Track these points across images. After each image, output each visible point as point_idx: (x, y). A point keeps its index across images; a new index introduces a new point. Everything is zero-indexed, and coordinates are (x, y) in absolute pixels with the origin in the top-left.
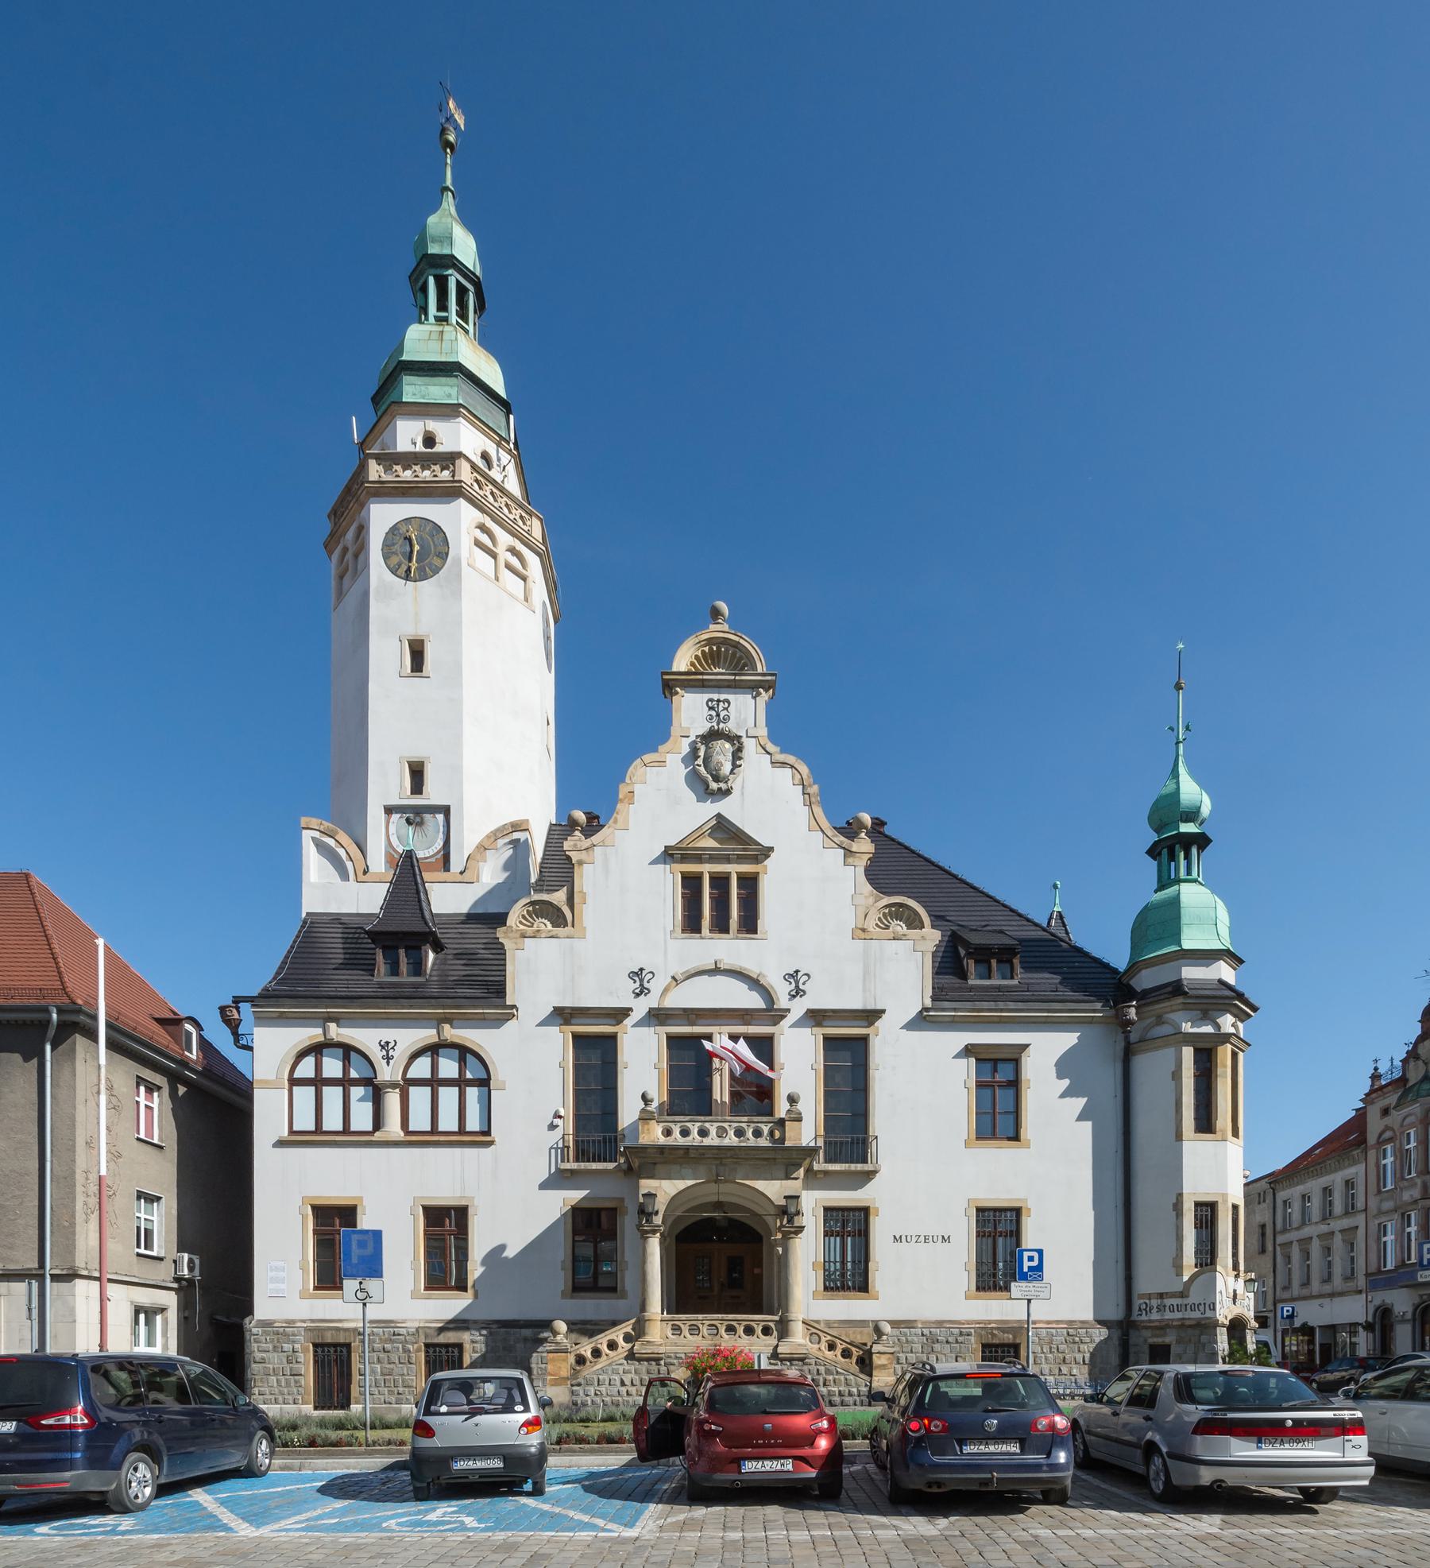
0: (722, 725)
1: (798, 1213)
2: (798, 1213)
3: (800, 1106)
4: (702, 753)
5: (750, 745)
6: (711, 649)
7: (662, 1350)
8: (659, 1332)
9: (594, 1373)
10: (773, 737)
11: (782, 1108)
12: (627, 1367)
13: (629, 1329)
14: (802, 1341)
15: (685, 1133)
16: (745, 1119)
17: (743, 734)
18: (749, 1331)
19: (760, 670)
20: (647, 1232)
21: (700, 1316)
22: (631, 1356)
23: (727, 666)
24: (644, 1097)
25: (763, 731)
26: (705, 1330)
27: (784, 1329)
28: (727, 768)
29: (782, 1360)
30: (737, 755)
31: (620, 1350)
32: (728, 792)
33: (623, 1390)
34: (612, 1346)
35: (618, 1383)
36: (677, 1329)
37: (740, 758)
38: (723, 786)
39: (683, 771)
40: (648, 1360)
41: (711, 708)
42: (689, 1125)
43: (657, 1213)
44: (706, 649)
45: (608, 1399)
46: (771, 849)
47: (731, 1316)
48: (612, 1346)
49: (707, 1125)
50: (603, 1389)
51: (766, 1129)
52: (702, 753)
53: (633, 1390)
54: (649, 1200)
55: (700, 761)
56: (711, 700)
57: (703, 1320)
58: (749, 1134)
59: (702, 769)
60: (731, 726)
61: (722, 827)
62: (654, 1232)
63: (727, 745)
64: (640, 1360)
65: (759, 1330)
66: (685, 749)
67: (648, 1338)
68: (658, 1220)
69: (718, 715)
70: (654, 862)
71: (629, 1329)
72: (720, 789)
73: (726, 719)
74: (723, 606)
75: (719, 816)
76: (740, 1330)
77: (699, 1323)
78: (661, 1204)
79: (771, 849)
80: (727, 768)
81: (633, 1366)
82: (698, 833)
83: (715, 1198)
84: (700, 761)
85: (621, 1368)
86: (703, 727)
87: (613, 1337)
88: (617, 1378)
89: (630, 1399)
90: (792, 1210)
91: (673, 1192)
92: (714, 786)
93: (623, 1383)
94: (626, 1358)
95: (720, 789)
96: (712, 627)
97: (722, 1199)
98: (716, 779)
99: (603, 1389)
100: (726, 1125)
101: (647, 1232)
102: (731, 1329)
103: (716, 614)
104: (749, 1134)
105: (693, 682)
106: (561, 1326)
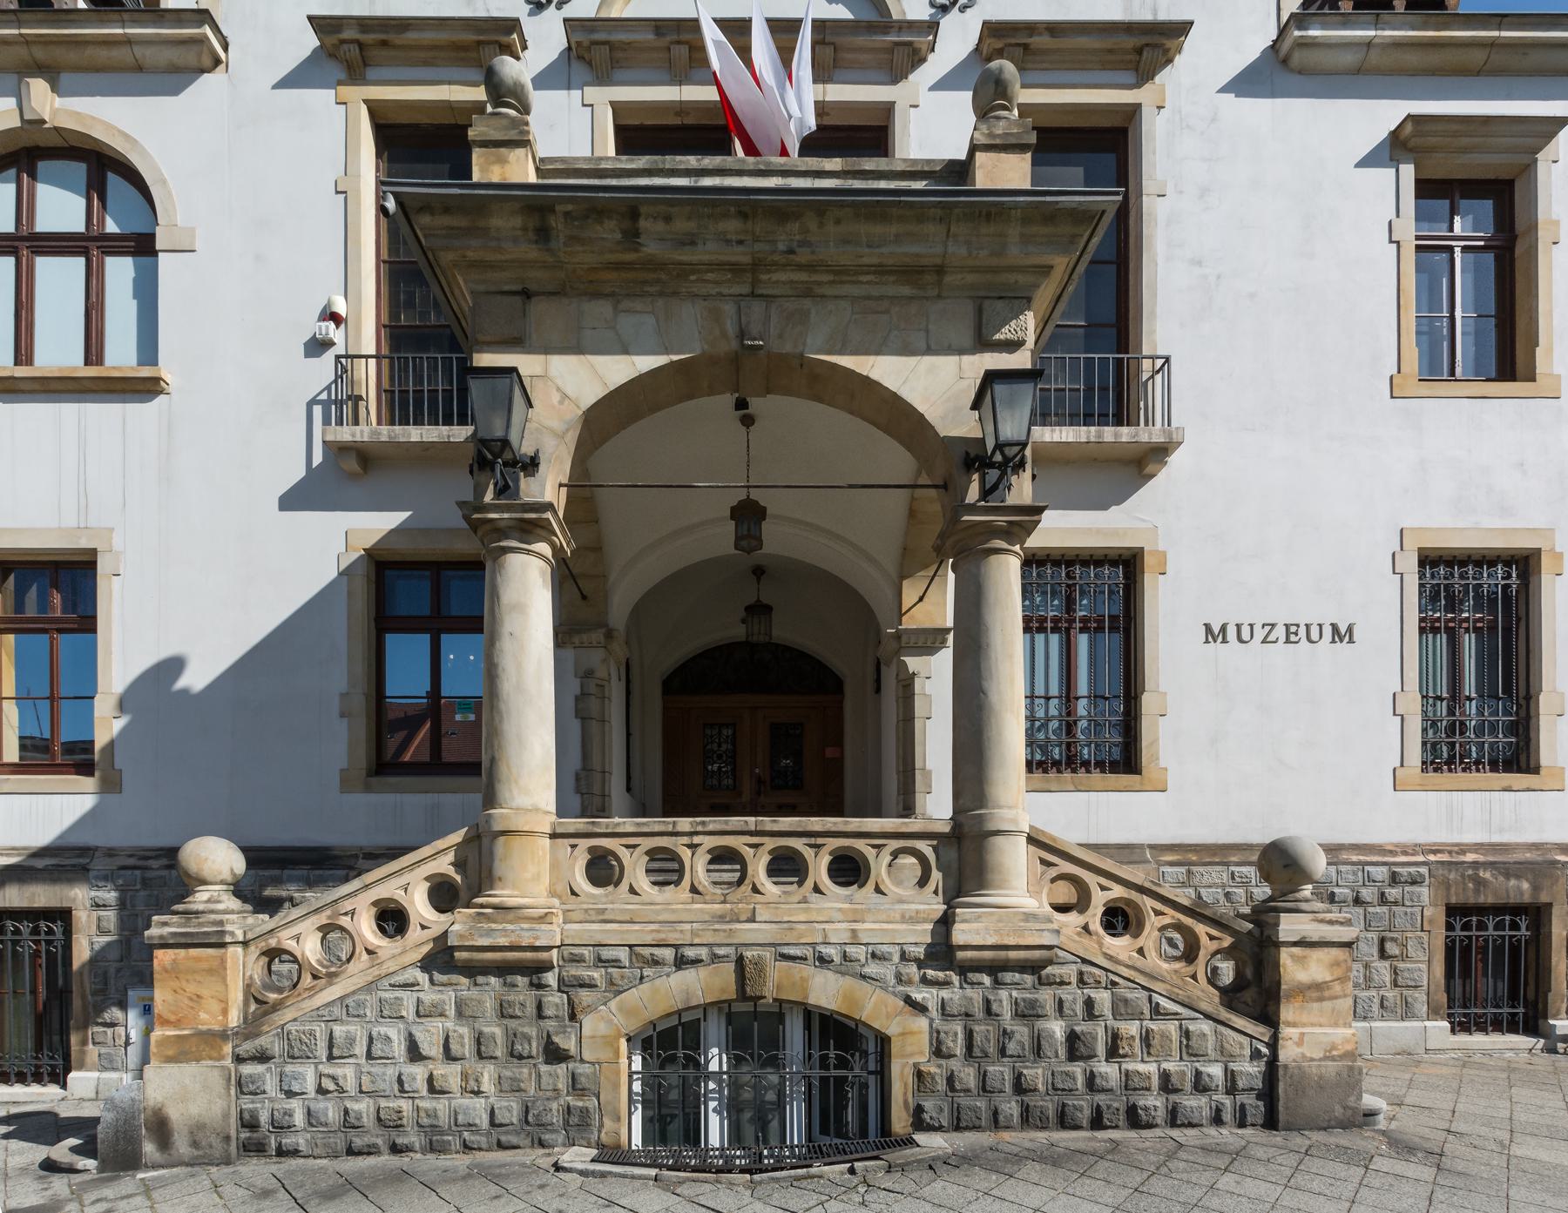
7: (551, 934)
8: (539, 879)
9: (318, 1015)
12: (429, 996)
13: (444, 865)
14: (1030, 904)
20: (500, 531)
21: (684, 823)
22: (441, 958)
26: (698, 867)
27: (963, 857)
29: (964, 970)
31: (414, 934)
33: (418, 1072)
34: (392, 919)
35: (399, 1049)
36: (602, 869)
40: (503, 970)
43: (531, 465)
45: (363, 1107)
47: (786, 822)
48: (392, 919)
50: (347, 1073)
53: (450, 1074)
57: (695, 837)
62: (530, 528)
64: (473, 971)
67: (503, 895)
71: (444, 865)
76: (819, 866)
77: (679, 845)
81: (446, 993)
85: (408, 999)
87: (389, 891)
88: (395, 1033)
89: (441, 1105)
91: (591, 394)
93: (415, 1053)
94: (427, 964)
99: (347, 1073)
101: (500, 531)
102: (787, 866)
106: (216, 858)
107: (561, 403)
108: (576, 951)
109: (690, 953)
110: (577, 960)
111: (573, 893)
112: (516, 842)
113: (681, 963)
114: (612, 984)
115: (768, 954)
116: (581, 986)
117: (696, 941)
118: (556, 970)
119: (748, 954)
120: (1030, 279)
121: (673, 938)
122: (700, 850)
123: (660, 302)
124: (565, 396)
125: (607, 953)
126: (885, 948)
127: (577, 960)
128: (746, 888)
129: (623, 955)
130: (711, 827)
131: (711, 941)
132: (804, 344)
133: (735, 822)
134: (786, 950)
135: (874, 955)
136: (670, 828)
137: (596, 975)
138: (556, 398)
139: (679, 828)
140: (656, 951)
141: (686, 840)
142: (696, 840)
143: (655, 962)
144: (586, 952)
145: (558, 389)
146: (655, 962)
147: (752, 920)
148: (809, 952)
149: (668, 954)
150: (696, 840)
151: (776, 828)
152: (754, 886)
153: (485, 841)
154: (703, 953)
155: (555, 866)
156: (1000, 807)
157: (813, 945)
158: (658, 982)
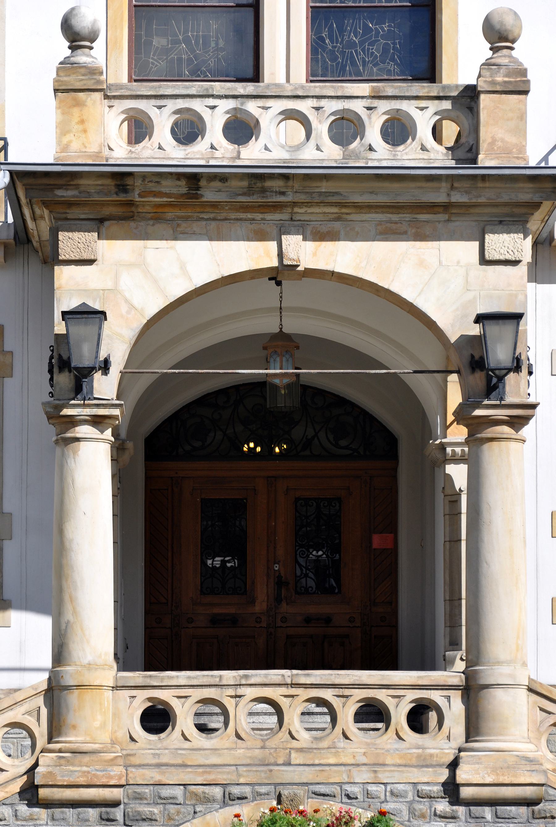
1: (517, 365)
2: (517, 365)
3: (522, 51)
11: (464, 58)
14: (526, 748)
15: (188, 130)
16: (364, 89)
18: (372, 713)
24: (76, 36)
42: (197, 105)
49: (252, 107)
51: (423, 119)
54: (80, 330)
58: (373, 134)
65: (399, 714)
68: (105, 386)
76: (347, 713)
78: (116, 342)
83: (269, 325)
90: (499, 355)
97: (293, 325)
100: (304, 106)
104: (373, 134)
107: (128, 312)
108: (139, 789)
109: (236, 791)
110: (139, 797)
111: (132, 739)
112: (88, 695)
113: (230, 799)
114: (170, 818)
115: (300, 791)
116: (144, 820)
117: (242, 781)
118: (122, 806)
119: (285, 792)
120: (523, 210)
121: (222, 778)
122: (243, 702)
123: (213, 224)
124: (132, 307)
125: (166, 792)
126: (401, 787)
127: (139, 797)
128: (283, 735)
129: (178, 792)
130: (252, 681)
131: (254, 781)
132: (335, 261)
133: (275, 675)
134: (318, 788)
135: (392, 793)
136: (216, 681)
137: (156, 811)
138: (124, 308)
139: (224, 682)
140: (206, 789)
141: (231, 692)
142: (240, 691)
143: (207, 800)
144: (146, 790)
145: (127, 301)
146: (207, 800)
147: (288, 764)
148: (336, 790)
149: (217, 792)
150: (240, 691)
151: (308, 681)
152: (290, 733)
153: (56, 693)
154: (247, 790)
155: (116, 715)
156: (499, 663)
157: (340, 784)
158: (208, 817)
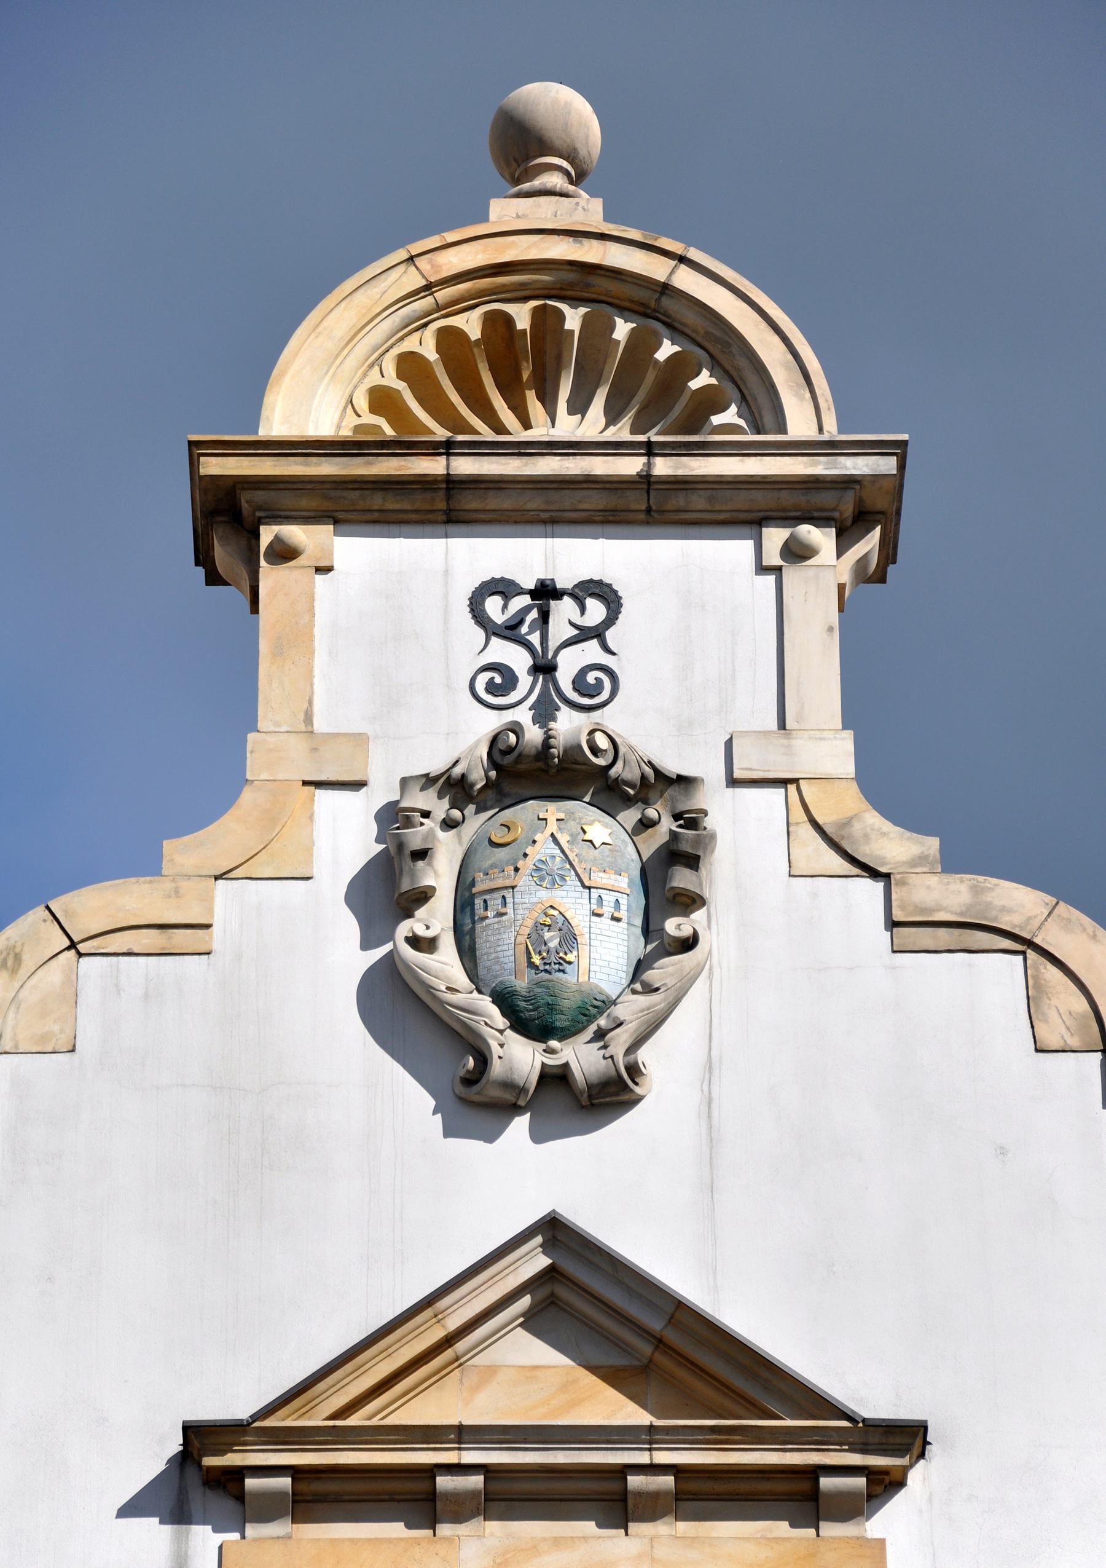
0: (568, 725)
4: (441, 876)
5: (745, 834)
6: (497, 324)
10: (876, 781)
17: (706, 766)
19: (800, 423)
23: (583, 397)
25: (828, 753)
28: (604, 954)
30: (670, 881)
32: (611, 1096)
37: (690, 902)
38: (581, 1057)
39: (349, 958)
41: (510, 631)
44: (471, 324)
46: (908, 1438)
52: (441, 876)
55: (436, 918)
56: (504, 588)
59: (444, 967)
60: (642, 726)
61: (576, 1287)
63: (601, 828)
66: (345, 835)
69: (544, 668)
70: (130, 1510)
72: (555, 1079)
73: (593, 690)
74: (564, 106)
75: (553, 1230)
79: (908, 1438)
80: (604, 954)
82: (428, 1336)
84: (436, 918)
86: (463, 734)
92: (520, 1057)
95: (555, 1079)
96: (504, 211)
98: (534, 1020)
103: (520, 149)
105: (389, 492)
